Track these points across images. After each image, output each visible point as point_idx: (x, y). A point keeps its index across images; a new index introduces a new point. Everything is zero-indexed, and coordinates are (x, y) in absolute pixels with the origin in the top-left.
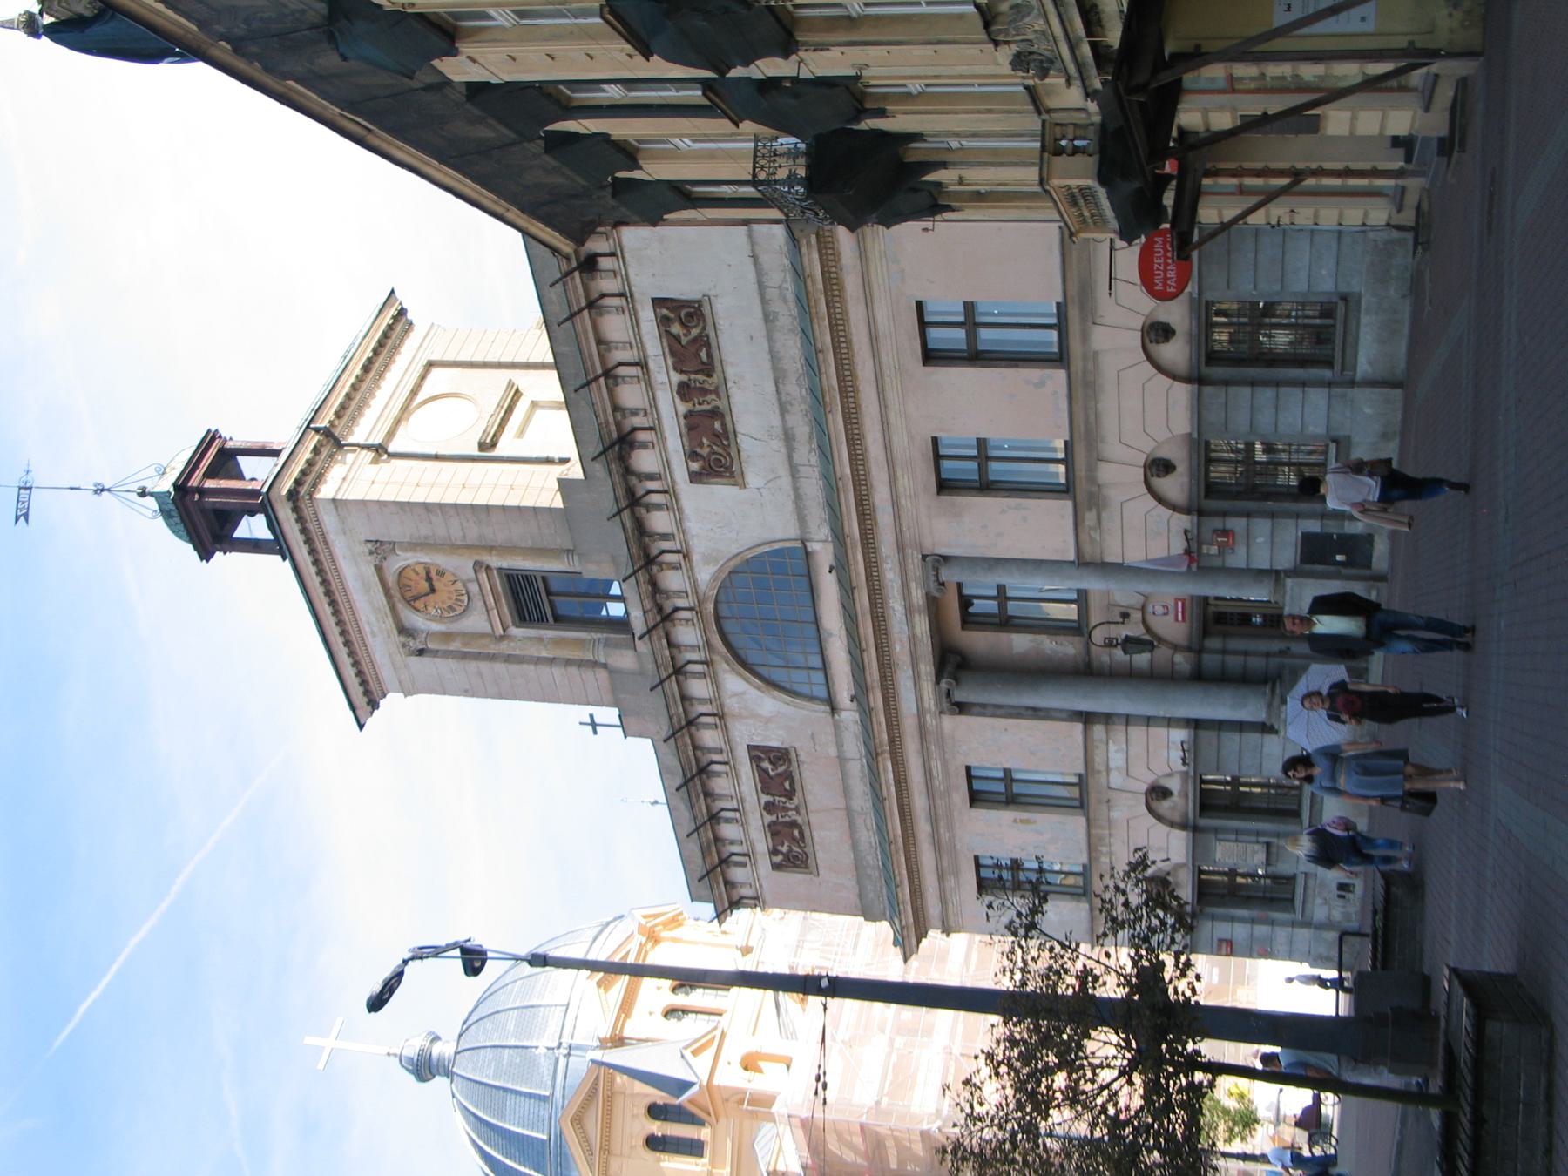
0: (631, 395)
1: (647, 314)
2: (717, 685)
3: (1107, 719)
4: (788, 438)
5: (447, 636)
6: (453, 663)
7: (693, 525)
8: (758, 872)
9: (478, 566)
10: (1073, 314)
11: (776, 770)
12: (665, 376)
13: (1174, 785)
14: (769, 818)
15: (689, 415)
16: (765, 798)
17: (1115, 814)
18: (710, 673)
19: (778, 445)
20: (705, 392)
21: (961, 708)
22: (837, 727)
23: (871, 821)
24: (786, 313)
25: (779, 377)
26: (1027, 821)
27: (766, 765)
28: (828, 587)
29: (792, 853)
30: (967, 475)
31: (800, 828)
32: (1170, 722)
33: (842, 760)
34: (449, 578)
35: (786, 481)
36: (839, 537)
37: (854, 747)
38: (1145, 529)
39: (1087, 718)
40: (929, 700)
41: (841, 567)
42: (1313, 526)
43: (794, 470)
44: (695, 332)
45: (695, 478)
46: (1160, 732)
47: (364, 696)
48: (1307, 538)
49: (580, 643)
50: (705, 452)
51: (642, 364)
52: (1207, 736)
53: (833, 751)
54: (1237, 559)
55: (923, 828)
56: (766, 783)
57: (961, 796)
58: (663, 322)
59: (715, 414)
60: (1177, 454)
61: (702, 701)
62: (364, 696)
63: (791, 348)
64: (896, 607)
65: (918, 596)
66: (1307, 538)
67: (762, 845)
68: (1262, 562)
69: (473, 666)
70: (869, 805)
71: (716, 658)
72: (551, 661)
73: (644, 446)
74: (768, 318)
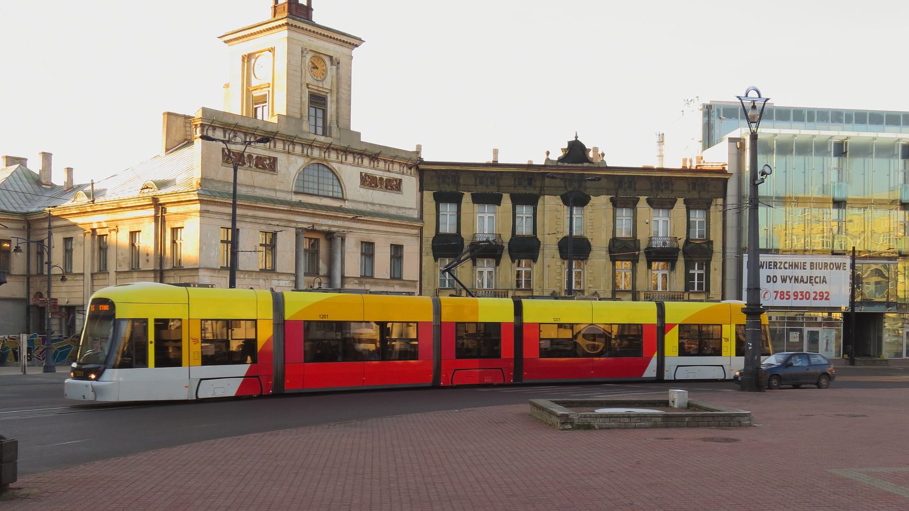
1: (399, 176)
7: (349, 167)
10: (401, 282)
11: (270, 165)
12: (386, 176)
16: (254, 156)
17: (261, 281)
18: (302, 155)
22: (288, 192)
23: (250, 194)
24: (401, 213)
28: (336, 204)
30: (368, 249)
33: (275, 190)
35: (361, 200)
36: (348, 211)
40: (300, 226)
41: (340, 209)
51: (389, 171)
53: (277, 188)
56: (260, 159)
58: (396, 180)
59: (376, 186)
61: (294, 148)
63: (393, 212)
64: (330, 222)
65: (333, 229)
74: (400, 208)
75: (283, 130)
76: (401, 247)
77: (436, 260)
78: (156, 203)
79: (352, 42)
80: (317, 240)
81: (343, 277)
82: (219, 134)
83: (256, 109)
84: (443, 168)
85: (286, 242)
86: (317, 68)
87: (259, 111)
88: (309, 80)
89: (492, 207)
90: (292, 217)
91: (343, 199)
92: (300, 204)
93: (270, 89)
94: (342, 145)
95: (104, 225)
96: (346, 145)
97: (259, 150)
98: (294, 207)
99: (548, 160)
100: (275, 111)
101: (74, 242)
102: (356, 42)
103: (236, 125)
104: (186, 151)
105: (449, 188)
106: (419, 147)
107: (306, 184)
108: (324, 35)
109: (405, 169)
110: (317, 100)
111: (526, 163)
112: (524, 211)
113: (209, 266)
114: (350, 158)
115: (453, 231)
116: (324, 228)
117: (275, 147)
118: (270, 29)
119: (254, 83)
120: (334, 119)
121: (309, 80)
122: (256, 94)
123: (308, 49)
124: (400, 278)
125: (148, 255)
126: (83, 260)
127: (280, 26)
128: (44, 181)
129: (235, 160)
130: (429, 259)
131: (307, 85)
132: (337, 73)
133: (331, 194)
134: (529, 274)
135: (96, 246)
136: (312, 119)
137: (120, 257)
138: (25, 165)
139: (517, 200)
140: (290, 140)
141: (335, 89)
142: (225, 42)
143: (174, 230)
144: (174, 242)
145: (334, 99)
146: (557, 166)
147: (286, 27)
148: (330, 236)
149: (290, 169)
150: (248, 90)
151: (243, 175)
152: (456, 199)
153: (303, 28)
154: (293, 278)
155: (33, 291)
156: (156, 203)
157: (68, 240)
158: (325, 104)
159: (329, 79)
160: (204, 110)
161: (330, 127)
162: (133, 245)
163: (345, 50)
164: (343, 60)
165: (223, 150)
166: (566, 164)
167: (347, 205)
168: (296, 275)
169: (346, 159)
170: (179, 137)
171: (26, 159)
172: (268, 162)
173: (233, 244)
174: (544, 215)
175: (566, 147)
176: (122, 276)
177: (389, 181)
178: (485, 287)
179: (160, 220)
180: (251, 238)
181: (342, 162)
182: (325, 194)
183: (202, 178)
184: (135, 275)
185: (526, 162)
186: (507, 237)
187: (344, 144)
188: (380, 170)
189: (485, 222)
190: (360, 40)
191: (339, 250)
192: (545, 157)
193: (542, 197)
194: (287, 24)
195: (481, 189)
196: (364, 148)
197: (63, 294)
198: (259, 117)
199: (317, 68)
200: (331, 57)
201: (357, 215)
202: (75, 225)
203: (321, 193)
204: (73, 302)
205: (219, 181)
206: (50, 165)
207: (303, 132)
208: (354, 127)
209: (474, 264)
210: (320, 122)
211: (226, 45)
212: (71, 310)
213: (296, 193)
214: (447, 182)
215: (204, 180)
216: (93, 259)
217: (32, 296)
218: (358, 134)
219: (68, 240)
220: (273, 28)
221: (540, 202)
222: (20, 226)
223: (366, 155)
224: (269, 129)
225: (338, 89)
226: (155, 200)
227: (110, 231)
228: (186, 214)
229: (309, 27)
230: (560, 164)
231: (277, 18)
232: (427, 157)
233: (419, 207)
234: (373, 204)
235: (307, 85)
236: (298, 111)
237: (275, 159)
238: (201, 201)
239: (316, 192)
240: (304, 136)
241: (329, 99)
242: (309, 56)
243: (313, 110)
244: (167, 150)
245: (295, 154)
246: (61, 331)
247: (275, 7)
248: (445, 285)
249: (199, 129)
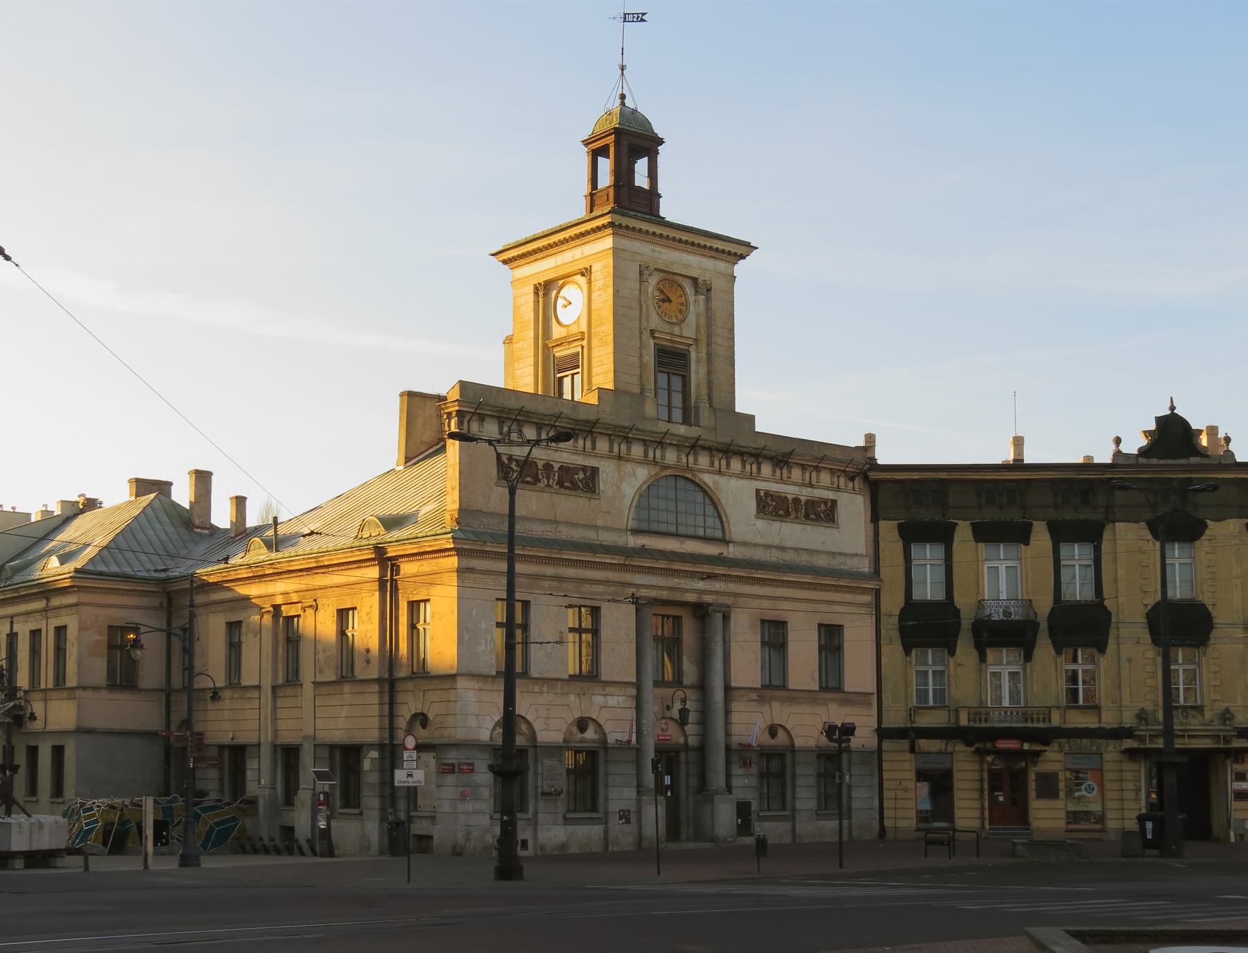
0: (796, 473)
1: (830, 495)
2: (639, 463)
7: (734, 482)
11: (583, 482)
12: (805, 494)
16: (556, 466)
17: (572, 697)
18: (645, 462)
19: (777, 542)
22: (619, 530)
24: (835, 563)
25: (812, 552)
28: (712, 550)
30: (774, 635)
31: (534, 483)
33: (596, 528)
35: (759, 540)
36: (734, 563)
38: (749, 723)
41: (718, 560)
42: (754, 807)
43: (768, 547)
45: (758, 491)
48: (749, 804)
51: (811, 485)
53: (600, 523)
54: (736, 770)
56: (566, 471)
58: (825, 501)
59: (788, 514)
61: (629, 449)
63: (821, 561)
64: (700, 585)
65: (708, 598)
66: (749, 804)
68: (735, 782)
70: (564, 537)
71: (658, 468)
73: (774, 472)
74: (833, 554)
75: (608, 417)
77: (907, 652)
78: (381, 556)
79: (736, 250)
80: (677, 620)
81: (728, 688)
82: (491, 429)
83: (561, 379)
84: (916, 476)
85: (619, 623)
86: (669, 301)
87: (567, 381)
88: (655, 322)
89: (1013, 549)
91: (724, 541)
92: (643, 552)
93: (585, 343)
94: (720, 439)
95: (294, 598)
96: (727, 440)
97: (564, 455)
98: (630, 558)
99: (1118, 454)
100: (594, 380)
101: (244, 630)
102: (740, 250)
103: (521, 411)
104: (438, 463)
105: (928, 514)
106: (870, 439)
107: (653, 514)
108: (680, 241)
109: (842, 480)
110: (671, 360)
111: (1080, 460)
112: (1077, 555)
113: (476, 671)
114: (736, 465)
115: (941, 596)
116: (691, 597)
117: (594, 447)
118: (582, 235)
119: (557, 332)
120: (704, 392)
121: (655, 322)
122: (560, 352)
123: (652, 266)
124: (839, 689)
125: (368, 651)
126: (257, 662)
127: (599, 229)
128: (197, 522)
129: (516, 474)
130: (893, 650)
131: (652, 332)
132: (708, 309)
133: (701, 532)
134: (1091, 678)
135: (281, 636)
136: (663, 395)
137: (321, 656)
138: (169, 495)
139: (1061, 533)
140: (622, 434)
141: (703, 338)
142: (505, 262)
143: (414, 606)
144: (413, 627)
145: (703, 355)
146: (1138, 465)
147: (610, 231)
148: (701, 611)
149: (624, 486)
150: (545, 347)
151: (530, 502)
152: (943, 535)
153: (640, 230)
154: (633, 691)
155: (176, 719)
156: (381, 556)
157: (234, 627)
158: (686, 366)
159: (692, 318)
160: (464, 386)
161: (697, 408)
162: (342, 633)
163: (722, 266)
164: (717, 284)
166: (1155, 461)
167: (732, 552)
168: (638, 686)
169: (728, 465)
170: (429, 435)
171: (170, 484)
172: (581, 476)
173: (515, 627)
174: (1115, 560)
175: (1152, 426)
176: (323, 690)
177: (812, 503)
178: (1006, 703)
179: (388, 586)
180: (551, 619)
181: (720, 472)
182: (691, 531)
183: (461, 510)
184: (347, 688)
185: (1079, 460)
186: (1044, 606)
187: (723, 438)
188: (794, 484)
189: (1000, 578)
190: (747, 245)
191: (719, 638)
192: (1113, 447)
193: (1109, 527)
194: (611, 224)
195: (989, 515)
196: (761, 443)
197: (225, 723)
198: (567, 395)
199: (669, 301)
200: (695, 280)
201: (754, 570)
202: (247, 598)
203: (682, 530)
204: (241, 739)
206: (209, 493)
207: (645, 419)
208: (740, 408)
209: (983, 658)
210: (677, 400)
211: (506, 267)
212: (238, 754)
213: (635, 532)
214: (926, 503)
215: (465, 513)
216: (275, 659)
217: (173, 727)
218: (750, 419)
219: (234, 627)
220: (587, 233)
221: (1107, 535)
222: (155, 602)
223: (766, 458)
224: (582, 417)
225: (709, 337)
226: (379, 550)
227: (304, 609)
228: (430, 579)
229: (652, 228)
230: (1142, 460)
231: (595, 214)
232: (885, 456)
233: (871, 552)
234: (782, 549)
235: (652, 332)
236: (635, 380)
237: (595, 471)
238: (460, 552)
239: (672, 529)
240: (649, 426)
241: (693, 356)
242: (653, 281)
243: (663, 378)
244: (407, 459)
245: (633, 461)
246: (221, 791)
247: (592, 195)
248: (927, 701)
249: (453, 422)
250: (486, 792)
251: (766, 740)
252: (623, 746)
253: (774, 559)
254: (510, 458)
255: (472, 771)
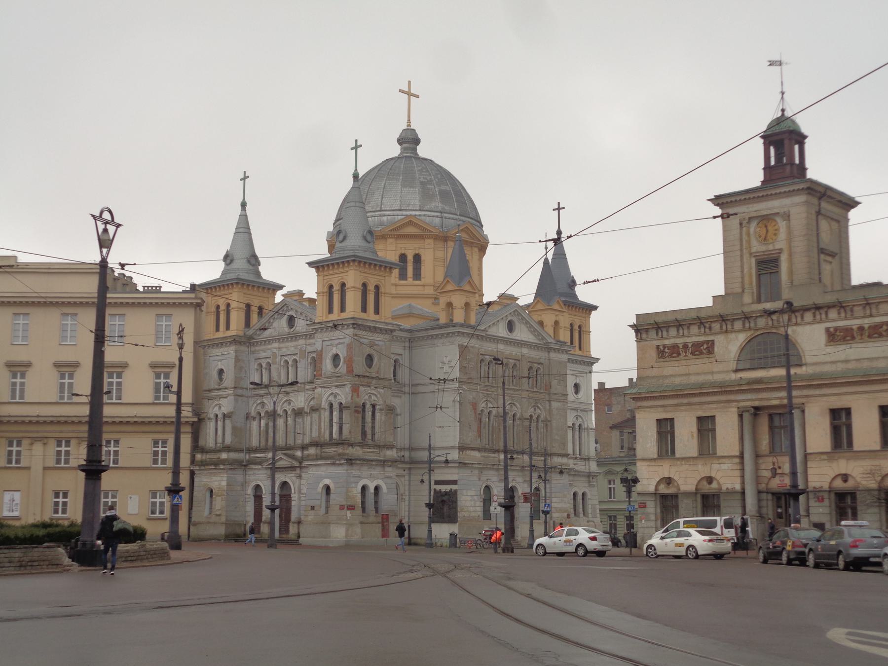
2: (739, 331)
3: (742, 463)
4: (847, 361)
5: (748, 234)
6: (738, 236)
7: (808, 327)
8: (654, 341)
9: (781, 249)
11: (705, 349)
12: (867, 322)
13: (714, 485)
14: (681, 346)
15: (852, 329)
16: (690, 345)
18: (744, 330)
20: (862, 335)
21: (741, 416)
26: (692, 436)
27: (705, 346)
29: (667, 353)
32: (743, 483)
33: (712, 373)
34: (774, 237)
37: (719, 378)
39: (741, 456)
40: (742, 404)
44: (884, 333)
45: (827, 330)
46: (738, 480)
47: (718, 201)
49: (751, 283)
50: (838, 333)
51: (871, 316)
52: (739, 497)
55: (685, 401)
56: (697, 346)
57: (701, 414)
59: (853, 338)
60: (850, 484)
62: (718, 201)
67: (666, 342)
69: (737, 243)
72: (742, 272)
76: (848, 411)
90: (732, 397)
113: (646, 457)
165: (658, 347)
205: (653, 377)
250: (653, 517)
251: (839, 484)
252: (731, 492)
253: (839, 369)
254: (664, 346)
255: (645, 507)
